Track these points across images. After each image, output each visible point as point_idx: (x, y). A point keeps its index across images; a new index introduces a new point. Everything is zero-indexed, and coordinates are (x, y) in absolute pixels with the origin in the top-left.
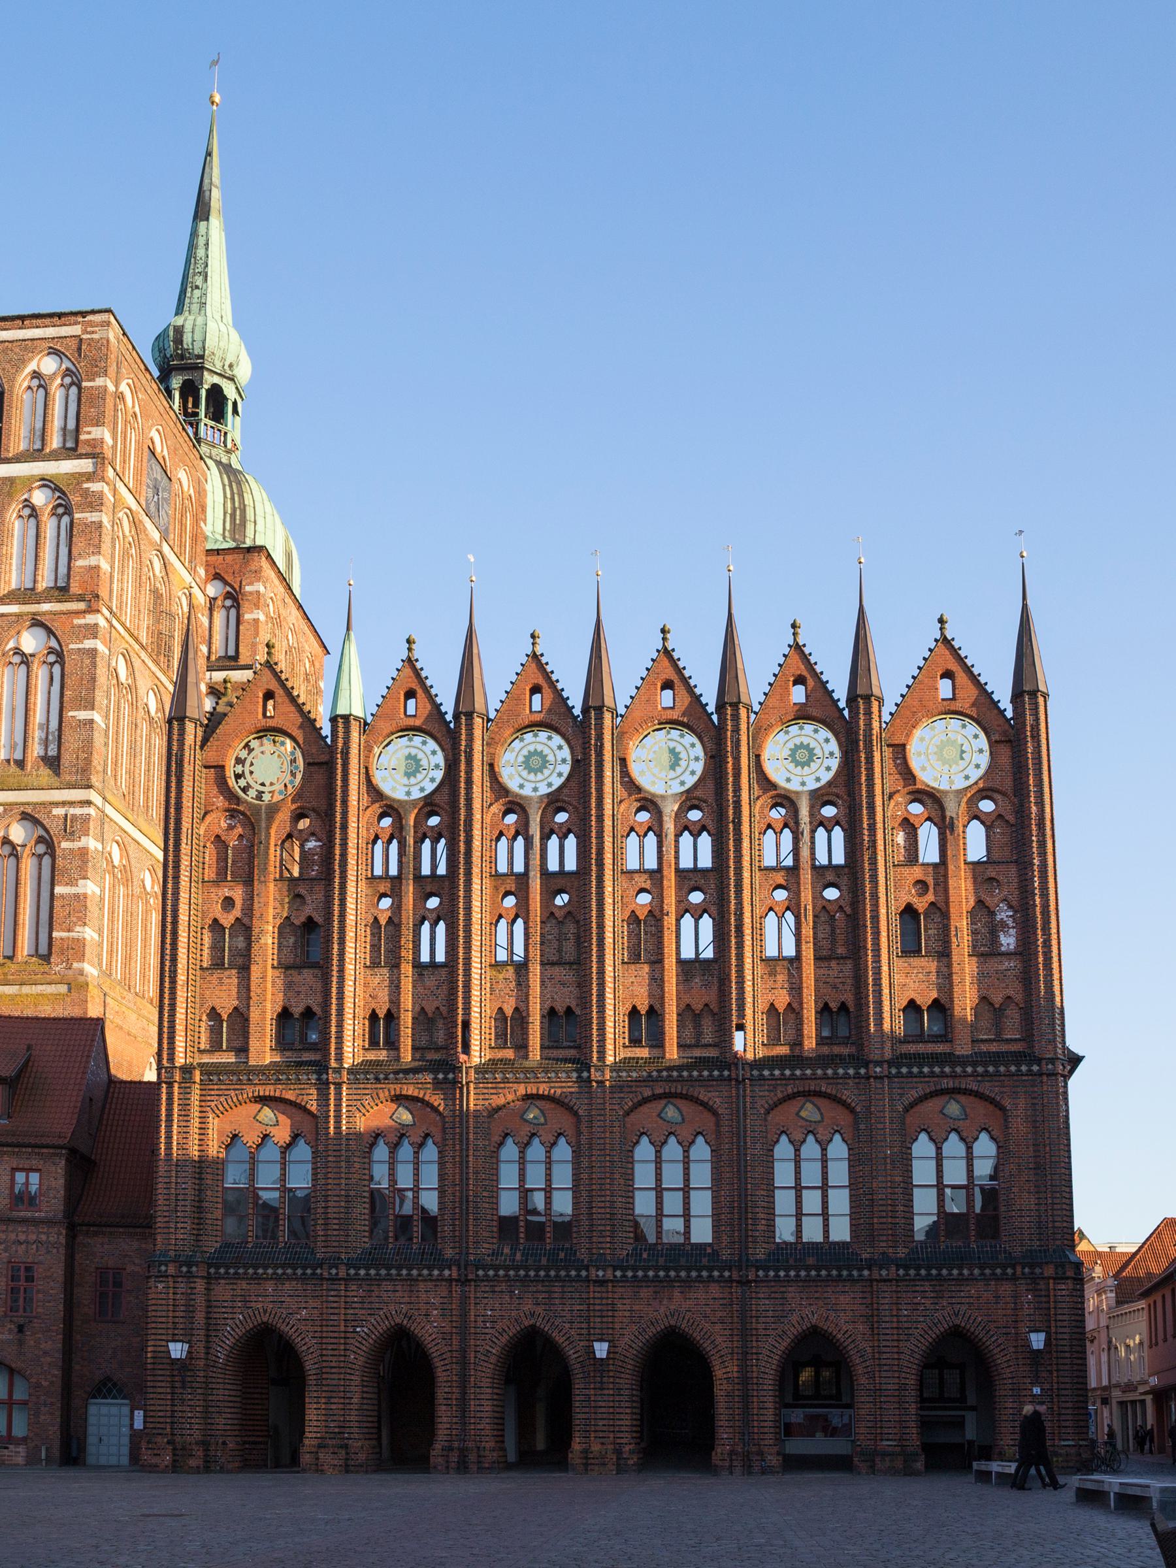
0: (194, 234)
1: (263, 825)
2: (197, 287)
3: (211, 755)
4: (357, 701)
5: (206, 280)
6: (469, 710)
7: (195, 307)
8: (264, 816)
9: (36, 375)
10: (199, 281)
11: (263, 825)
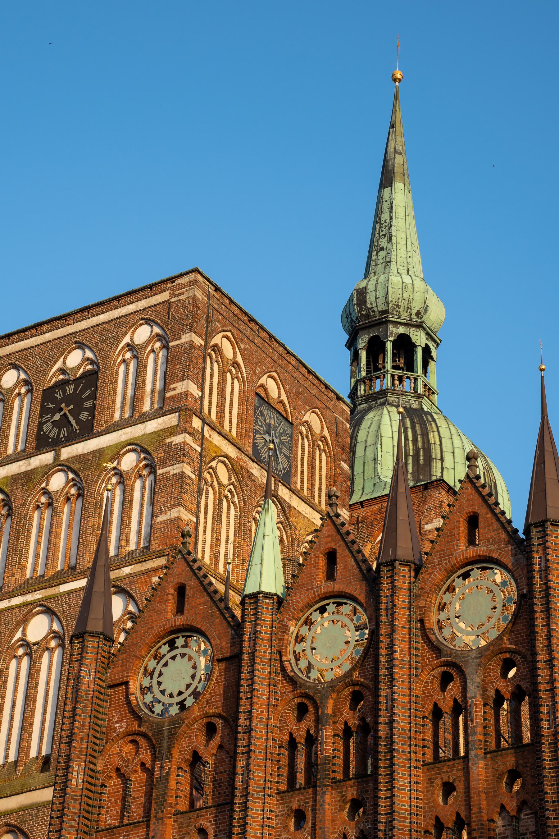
0: (380, 201)
1: (165, 745)
2: (382, 249)
3: (114, 674)
4: (269, 576)
5: (390, 240)
6: (390, 557)
7: (380, 268)
8: (166, 733)
9: (130, 347)
10: (384, 243)
11: (165, 745)
